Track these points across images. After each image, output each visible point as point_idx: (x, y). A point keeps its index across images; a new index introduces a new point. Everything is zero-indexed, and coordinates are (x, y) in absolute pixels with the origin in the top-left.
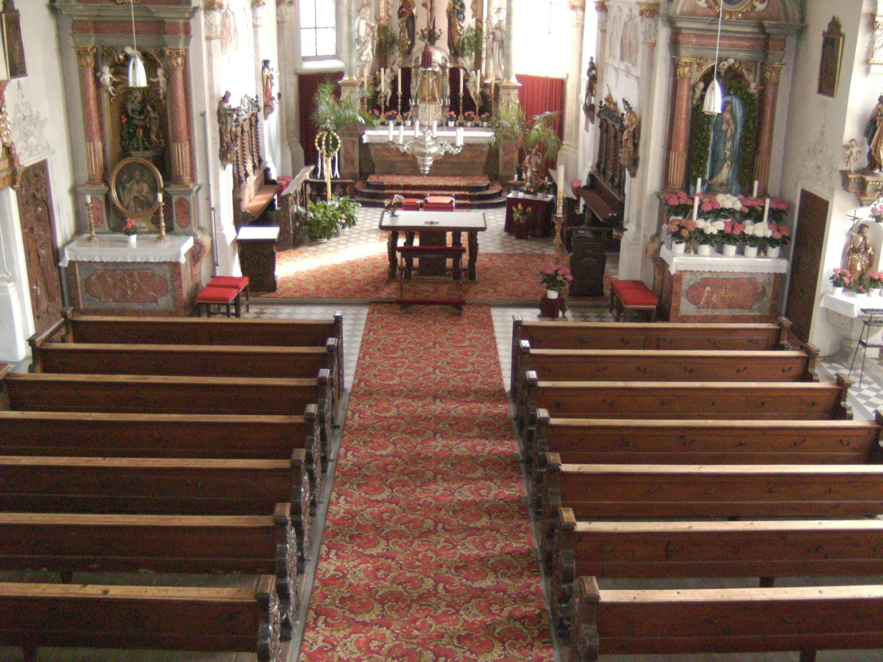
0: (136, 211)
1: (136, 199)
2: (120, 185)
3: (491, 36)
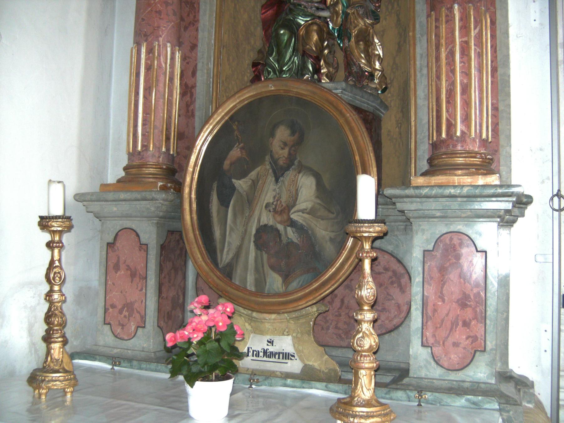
0: (260, 282)
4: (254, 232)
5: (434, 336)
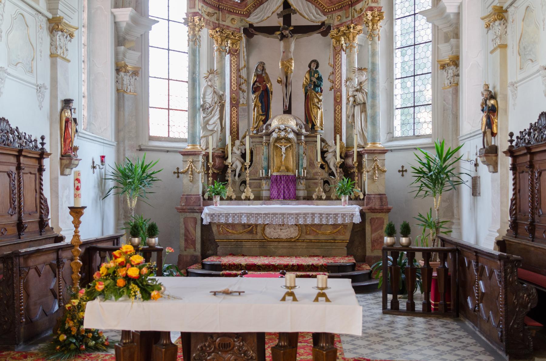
3: (351, 99)
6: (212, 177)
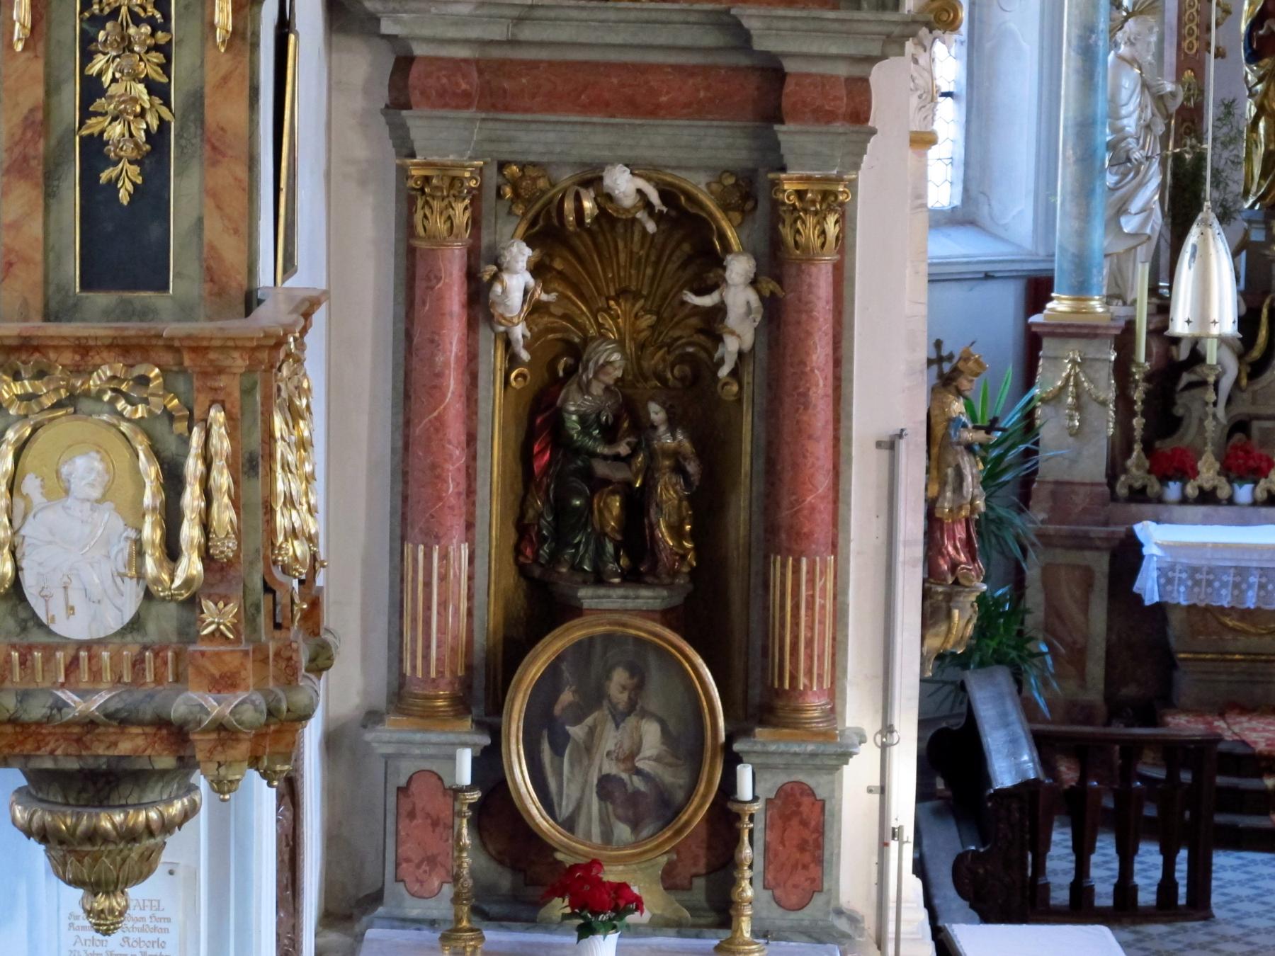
1: (606, 786)
2: (544, 727)
4: (595, 781)
5: (775, 879)
6: (1144, 414)
